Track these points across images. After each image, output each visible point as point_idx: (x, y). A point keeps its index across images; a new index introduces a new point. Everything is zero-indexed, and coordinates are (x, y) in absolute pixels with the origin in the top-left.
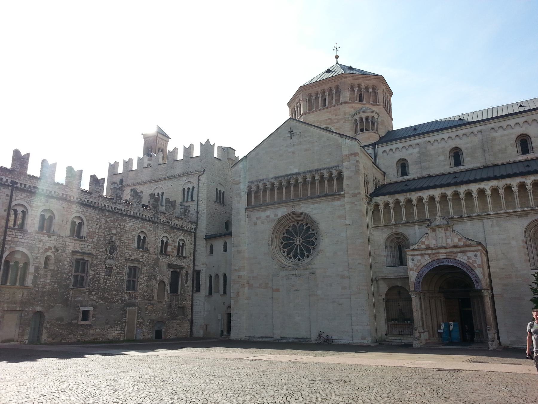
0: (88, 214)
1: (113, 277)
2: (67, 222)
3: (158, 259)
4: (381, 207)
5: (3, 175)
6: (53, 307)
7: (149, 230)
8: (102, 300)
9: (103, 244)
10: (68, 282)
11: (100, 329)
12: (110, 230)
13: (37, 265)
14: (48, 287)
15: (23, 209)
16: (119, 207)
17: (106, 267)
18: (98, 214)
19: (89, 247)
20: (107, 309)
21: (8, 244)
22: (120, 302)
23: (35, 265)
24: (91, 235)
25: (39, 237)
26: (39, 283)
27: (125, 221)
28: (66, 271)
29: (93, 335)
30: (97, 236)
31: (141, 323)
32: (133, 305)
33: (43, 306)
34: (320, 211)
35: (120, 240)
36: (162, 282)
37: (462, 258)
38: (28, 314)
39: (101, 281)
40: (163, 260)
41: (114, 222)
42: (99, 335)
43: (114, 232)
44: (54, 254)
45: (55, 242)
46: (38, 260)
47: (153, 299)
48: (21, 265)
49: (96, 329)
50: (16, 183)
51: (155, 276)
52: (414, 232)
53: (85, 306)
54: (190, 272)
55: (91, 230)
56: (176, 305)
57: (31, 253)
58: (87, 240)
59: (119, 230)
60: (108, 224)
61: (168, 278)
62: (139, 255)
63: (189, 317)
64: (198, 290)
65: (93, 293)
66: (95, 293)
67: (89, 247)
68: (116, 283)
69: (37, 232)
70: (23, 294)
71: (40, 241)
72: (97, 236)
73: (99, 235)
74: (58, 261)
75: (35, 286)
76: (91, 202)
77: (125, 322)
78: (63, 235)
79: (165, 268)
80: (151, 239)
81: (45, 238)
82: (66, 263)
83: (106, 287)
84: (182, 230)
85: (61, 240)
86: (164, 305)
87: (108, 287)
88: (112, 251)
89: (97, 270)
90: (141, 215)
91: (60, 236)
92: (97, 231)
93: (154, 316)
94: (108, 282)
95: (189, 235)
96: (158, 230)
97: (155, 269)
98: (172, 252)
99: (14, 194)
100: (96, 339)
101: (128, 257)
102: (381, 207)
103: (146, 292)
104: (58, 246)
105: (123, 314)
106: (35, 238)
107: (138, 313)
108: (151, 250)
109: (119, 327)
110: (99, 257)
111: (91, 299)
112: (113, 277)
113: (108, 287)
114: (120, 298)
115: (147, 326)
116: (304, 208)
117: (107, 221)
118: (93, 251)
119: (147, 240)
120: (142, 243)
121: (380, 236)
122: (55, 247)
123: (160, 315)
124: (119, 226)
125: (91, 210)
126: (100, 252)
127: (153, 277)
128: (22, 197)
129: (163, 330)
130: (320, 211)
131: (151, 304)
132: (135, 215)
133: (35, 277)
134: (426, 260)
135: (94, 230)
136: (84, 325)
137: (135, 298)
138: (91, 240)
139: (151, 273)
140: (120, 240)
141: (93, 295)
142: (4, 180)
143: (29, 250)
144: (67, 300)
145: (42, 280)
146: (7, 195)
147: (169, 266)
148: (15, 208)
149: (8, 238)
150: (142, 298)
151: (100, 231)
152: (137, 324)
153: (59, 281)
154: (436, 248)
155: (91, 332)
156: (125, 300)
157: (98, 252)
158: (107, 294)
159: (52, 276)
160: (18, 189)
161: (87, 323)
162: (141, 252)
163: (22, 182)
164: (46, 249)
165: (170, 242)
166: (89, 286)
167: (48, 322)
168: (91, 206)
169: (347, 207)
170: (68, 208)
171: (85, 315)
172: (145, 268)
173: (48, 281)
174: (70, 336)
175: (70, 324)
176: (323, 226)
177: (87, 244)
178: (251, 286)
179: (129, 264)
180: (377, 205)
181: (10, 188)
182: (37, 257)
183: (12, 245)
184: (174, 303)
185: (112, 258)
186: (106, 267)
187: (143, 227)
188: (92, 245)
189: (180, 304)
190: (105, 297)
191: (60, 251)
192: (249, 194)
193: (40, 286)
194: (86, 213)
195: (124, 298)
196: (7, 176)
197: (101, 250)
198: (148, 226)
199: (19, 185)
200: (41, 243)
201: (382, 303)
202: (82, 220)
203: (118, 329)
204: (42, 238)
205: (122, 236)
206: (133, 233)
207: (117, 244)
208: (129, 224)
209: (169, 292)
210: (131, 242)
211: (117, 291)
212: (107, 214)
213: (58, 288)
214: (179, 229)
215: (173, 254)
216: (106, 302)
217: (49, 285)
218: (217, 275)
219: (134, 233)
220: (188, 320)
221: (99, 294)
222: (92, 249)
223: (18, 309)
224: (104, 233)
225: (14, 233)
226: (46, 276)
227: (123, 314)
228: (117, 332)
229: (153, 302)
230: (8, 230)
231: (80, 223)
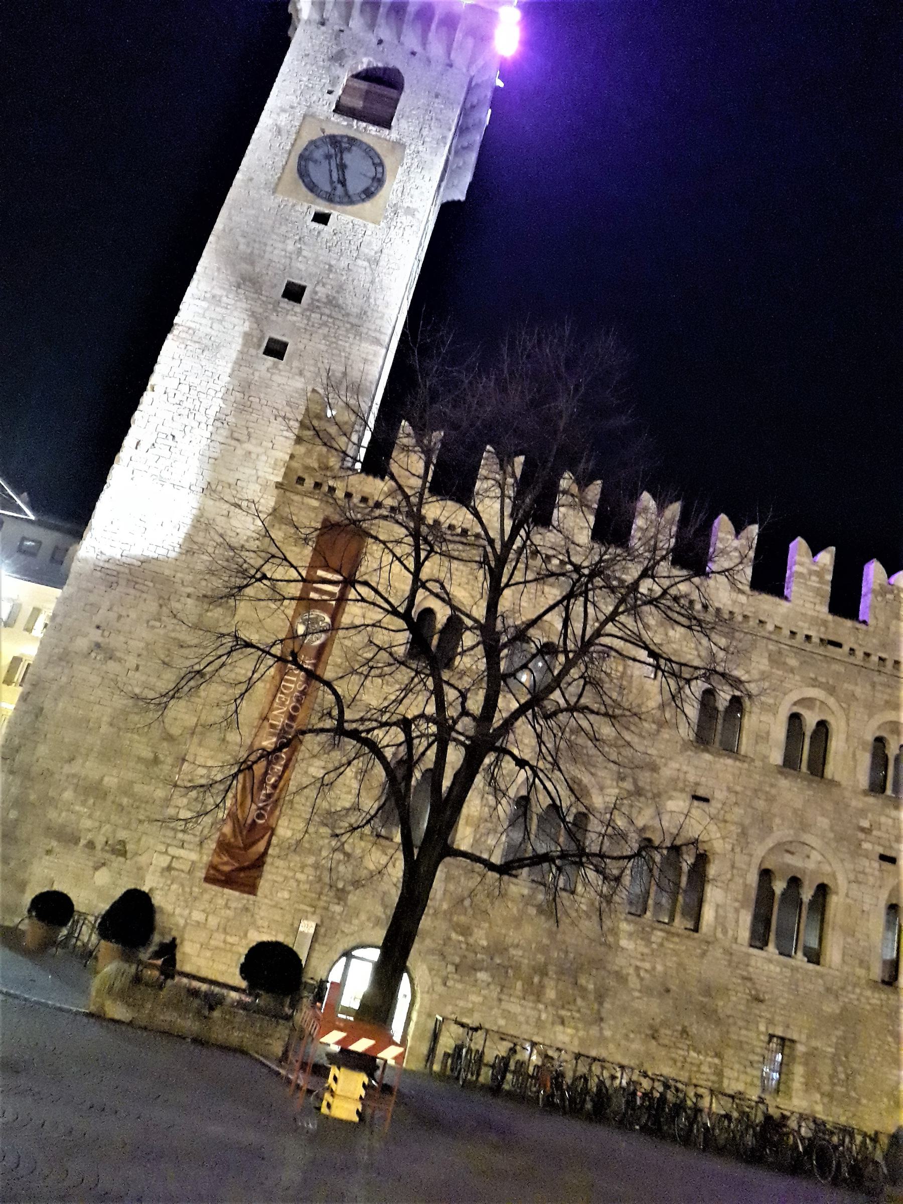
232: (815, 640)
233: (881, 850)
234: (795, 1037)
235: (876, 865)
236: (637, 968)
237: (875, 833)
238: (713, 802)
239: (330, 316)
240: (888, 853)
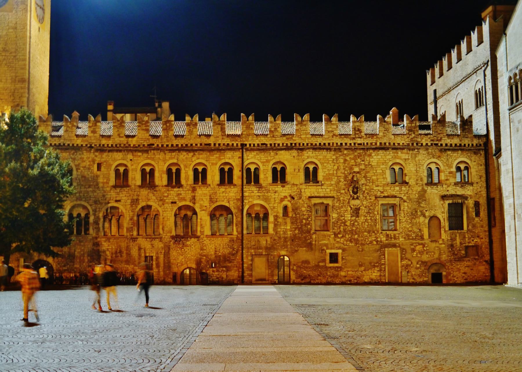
0: (321, 157)
1: (362, 218)
2: (299, 170)
3: (425, 191)
5: (233, 141)
6: (297, 251)
7: (405, 159)
8: (351, 242)
9: (345, 185)
10: (309, 227)
11: (353, 271)
12: (351, 168)
13: (275, 214)
14: (289, 233)
15: (255, 166)
16: (359, 141)
17: (351, 208)
18: (334, 155)
19: (328, 190)
20: (359, 251)
21: (246, 199)
22: (375, 243)
23: (273, 214)
24: (328, 178)
25: (274, 189)
26: (279, 230)
27: (370, 155)
28: (305, 217)
29: (345, 277)
30: (336, 178)
31: (407, 265)
32: (394, 246)
33: (287, 251)
35: (365, 177)
38: (274, 257)
39: (348, 223)
40: (433, 193)
41: (355, 159)
42: (352, 277)
43: (356, 169)
44: (291, 202)
45: (290, 191)
46: (276, 210)
47: (422, 238)
48: (261, 215)
49: (348, 271)
50: (246, 145)
51: (421, 211)
53: (331, 249)
54: (483, 201)
55: (327, 172)
56: (461, 243)
57: (268, 204)
58: (325, 184)
59: (363, 167)
60: (347, 162)
61: (443, 213)
62: (395, 190)
63: (487, 258)
65: (340, 236)
66: (341, 235)
67: (327, 190)
68: (366, 224)
69: (270, 185)
70: (267, 241)
71: (275, 192)
72: (336, 178)
73: (338, 177)
75: (276, 233)
76: (325, 144)
77: (384, 264)
78: (297, 183)
79: (437, 201)
80: (410, 169)
81: (279, 188)
82: (303, 209)
83: (354, 228)
84: (462, 150)
85: (296, 188)
86: (441, 244)
87: (357, 228)
88: (355, 190)
89: (340, 212)
90: (392, 144)
91: (294, 184)
92: (335, 172)
93: (425, 257)
94: (356, 224)
95: (475, 153)
96: (419, 157)
97: (419, 203)
98: (447, 180)
99: (245, 155)
100: (350, 281)
101: (379, 194)
103: (411, 231)
104: (293, 194)
105: (380, 256)
106: (269, 190)
107: (402, 254)
108: (412, 182)
109: (377, 269)
110: (341, 198)
111: (337, 242)
112: (362, 218)
113: (357, 228)
114: (374, 239)
115: (417, 268)
117: (345, 160)
118: (333, 194)
119: (405, 172)
122: (290, 196)
123: (436, 256)
124: (363, 162)
125: (324, 152)
126: (341, 194)
127: (419, 213)
128: (253, 156)
129: (444, 273)
131: (419, 244)
132: (383, 146)
133: (275, 225)
135: (331, 172)
136: (334, 267)
137: (395, 238)
138: (329, 183)
139: (415, 209)
140: (365, 177)
141: (339, 238)
142: (235, 145)
143: (266, 202)
144: (311, 244)
145: (282, 227)
146: (239, 157)
147: (444, 197)
148: (249, 166)
149: (246, 194)
150: (405, 238)
151: (339, 172)
152: (402, 266)
153: (300, 226)
155: (343, 274)
156: (381, 241)
157: (339, 194)
158: (356, 236)
159: (292, 223)
160: (247, 150)
161: (336, 265)
162: (397, 186)
163: (250, 143)
164: (282, 198)
165: (442, 168)
166: (333, 229)
167: (294, 265)
168: (324, 149)
170: (298, 156)
171: (334, 258)
172: (406, 204)
173: (289, 228)
174: (319, 277)
175: (317, 266)
177: (326, 187)
179: (381, 202)
181: (241, 150)
182: (274, 207)
183: (250, 200)
184: (458, 241)
185: (357, 198)
186: (351, 208)
187: (396, 157)
188: (331, 188)
189: (469, 243)
190: (354, 239)
191: (296, 198)
193: (281, 233)
194: (319, 157)
195: (379, 239)
196: (237, 141)
197: (343, 192)
198: (403, 155)
199: (248, 146)
200: (277, 194)
202: (316, 165)
203: (375, 271)
204: (277, 189)
205: (368, 172)
206: (381, 166)
207: (363, 181)
208: (375, 157)
209: (447, 228)
210: (382, 177)
211: (369, 232)
212: (345, 152)
213: (299, 234)
214: (454, 150)
215: (448, 182)
216: (356, 244)
217: (291, 231)
219: (384, 166)
220: (486, 261)
221: (347, 236)
222: (332, 192)
223: (264, 254)
224: (344, 173)
225: (250, 189)
226: (286, 223)
227: (380, 256)
228: (375, 274)
229: (423, 242)
230: (244, 187)
231: (314, 168)
232: (146, 145)
233: (171, 201)
234: (152, 255)
235: (170, 205)
236: (108, 249)
237: (169, 196)
238: (122, 201)
239: (5, 56)
240: (174, 201)
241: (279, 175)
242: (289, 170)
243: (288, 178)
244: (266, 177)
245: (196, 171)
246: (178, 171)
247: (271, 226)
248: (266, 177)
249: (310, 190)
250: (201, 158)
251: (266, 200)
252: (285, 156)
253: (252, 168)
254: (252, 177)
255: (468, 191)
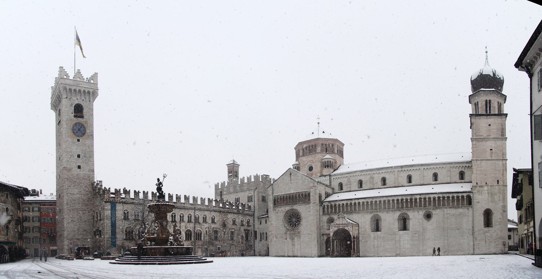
4: (326, 207)
32: (233, 245)
34: (300, 208)
36: (242, 236)
37: (346, 228)
52: (335, 217)
62: (234, 227)
64: (256, 239)
74: (209, 231)
80: (237, 220)
93: (240, 249)
102: (326, 207)
116: (295, 207)
120: (234, 223)
121: (325, 218)
130: (300, 208)
134: (336, 229)
154: (339, 224)
169: (312, 207)
176: (303, 215)
178: (276, 237)
180: (324, 206)
192: (275, 201)
201: (324, 243)
218: (263, 233)
241: (205, 220)
242: (208, 218)
243: (207, 221)
244: (201, 220)
245: (180, 216)
246: (175, 216)
247: (202, 237)
248: (201, 220)
249: (213, 226)
250: (182, 212)
251: (201, 228)
252: (206, 213)
253: (197, 216)
254: (197, 220)
255: (249, 228)
